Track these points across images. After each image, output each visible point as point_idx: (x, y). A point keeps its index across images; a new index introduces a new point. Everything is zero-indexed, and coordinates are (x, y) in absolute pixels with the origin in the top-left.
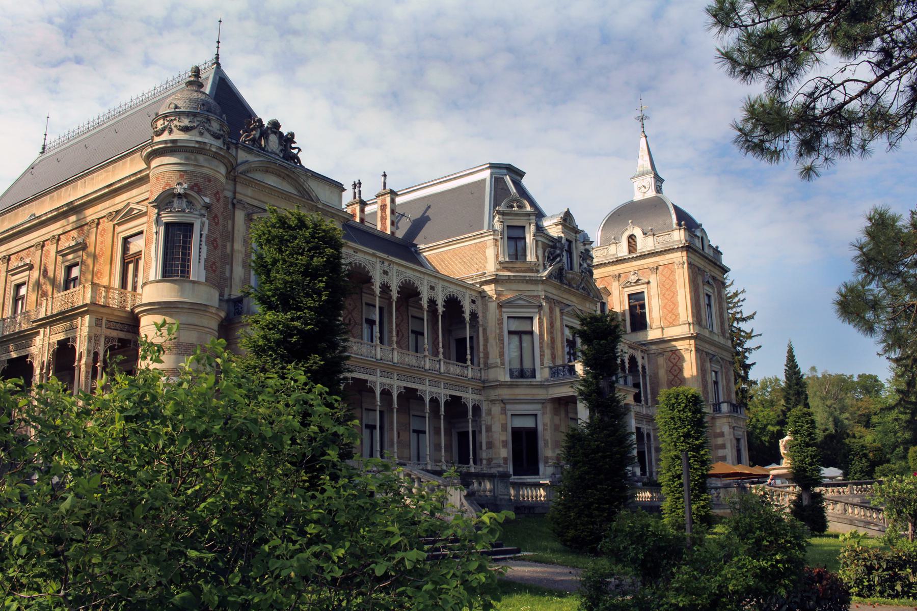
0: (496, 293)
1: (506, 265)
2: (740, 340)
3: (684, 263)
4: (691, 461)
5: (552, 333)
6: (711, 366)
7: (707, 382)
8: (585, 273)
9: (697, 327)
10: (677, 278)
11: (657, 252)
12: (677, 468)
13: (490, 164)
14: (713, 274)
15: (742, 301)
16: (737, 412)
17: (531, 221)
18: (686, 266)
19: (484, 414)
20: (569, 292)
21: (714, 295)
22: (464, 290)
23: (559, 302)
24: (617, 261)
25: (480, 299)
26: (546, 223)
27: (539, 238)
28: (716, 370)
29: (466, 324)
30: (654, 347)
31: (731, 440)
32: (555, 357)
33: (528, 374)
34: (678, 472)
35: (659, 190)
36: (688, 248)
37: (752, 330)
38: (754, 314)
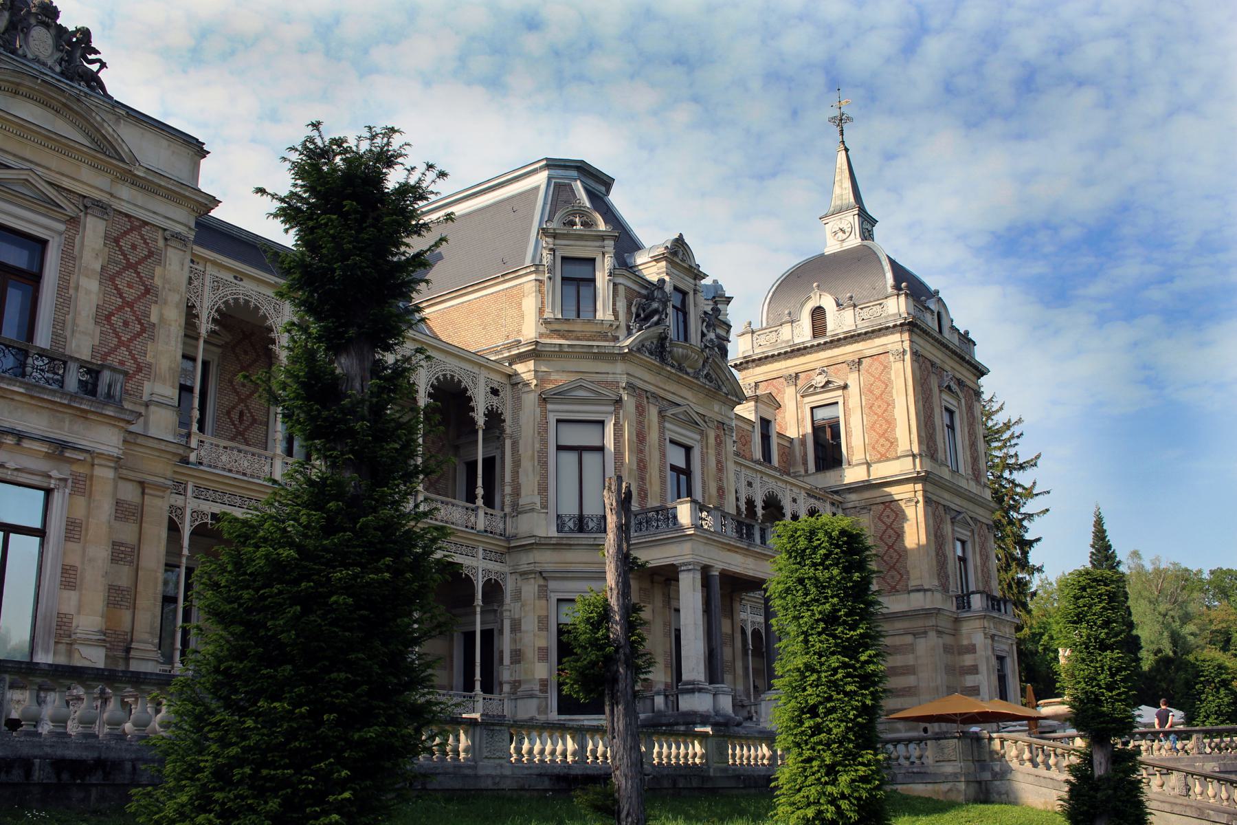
0: (536, 377)
1: (556, 327)
2: (1014, 500)
3: (904, 352)
4: (839, 676)
5: (641, 451)
6: (953, 530)
7: (945, 557)
8: (712, 349)
9: (927, 461)
10: (893, 378)
11: (859, 335)
12: (810, 691)
13: (547, 159)
14: (958, 376)
15: (1018, 437)
16: (999, 610)
17: (606, 249)
18: (908, 357)
19: (508, 599)
20: (679, 381)
21: (960, 412)
22: (476, 370)
23: (655, 396)
24: (792, 351)
25: (508, 387)
26: (641, 259)
27: (619, 280)
28: (964, 538)
29: (477, 431)
30: (853, 497)
32: (646, 495)
33: (591, 525)
34: (811, 702)
35: (867, 234)
36: (911, 326)
37: (1034, 483)
38: (1038, 457)
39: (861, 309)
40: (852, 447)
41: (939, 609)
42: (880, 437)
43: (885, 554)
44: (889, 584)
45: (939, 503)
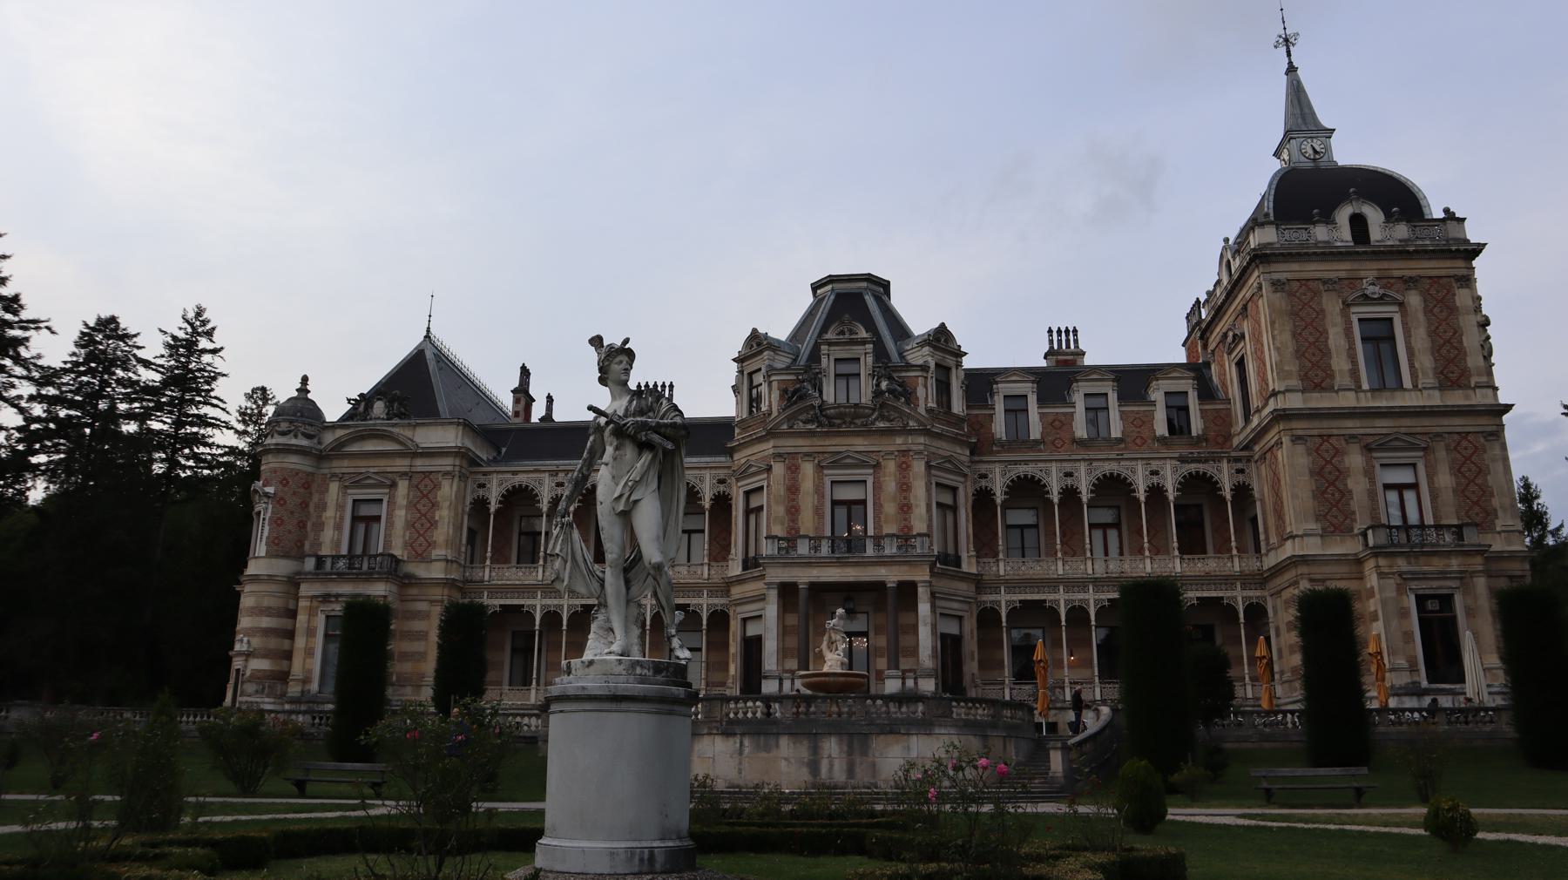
3: (1260, 288)
7: (1346, 494)
30: (1257, 448)
31: (1384, 603)
45: (1330, 436)
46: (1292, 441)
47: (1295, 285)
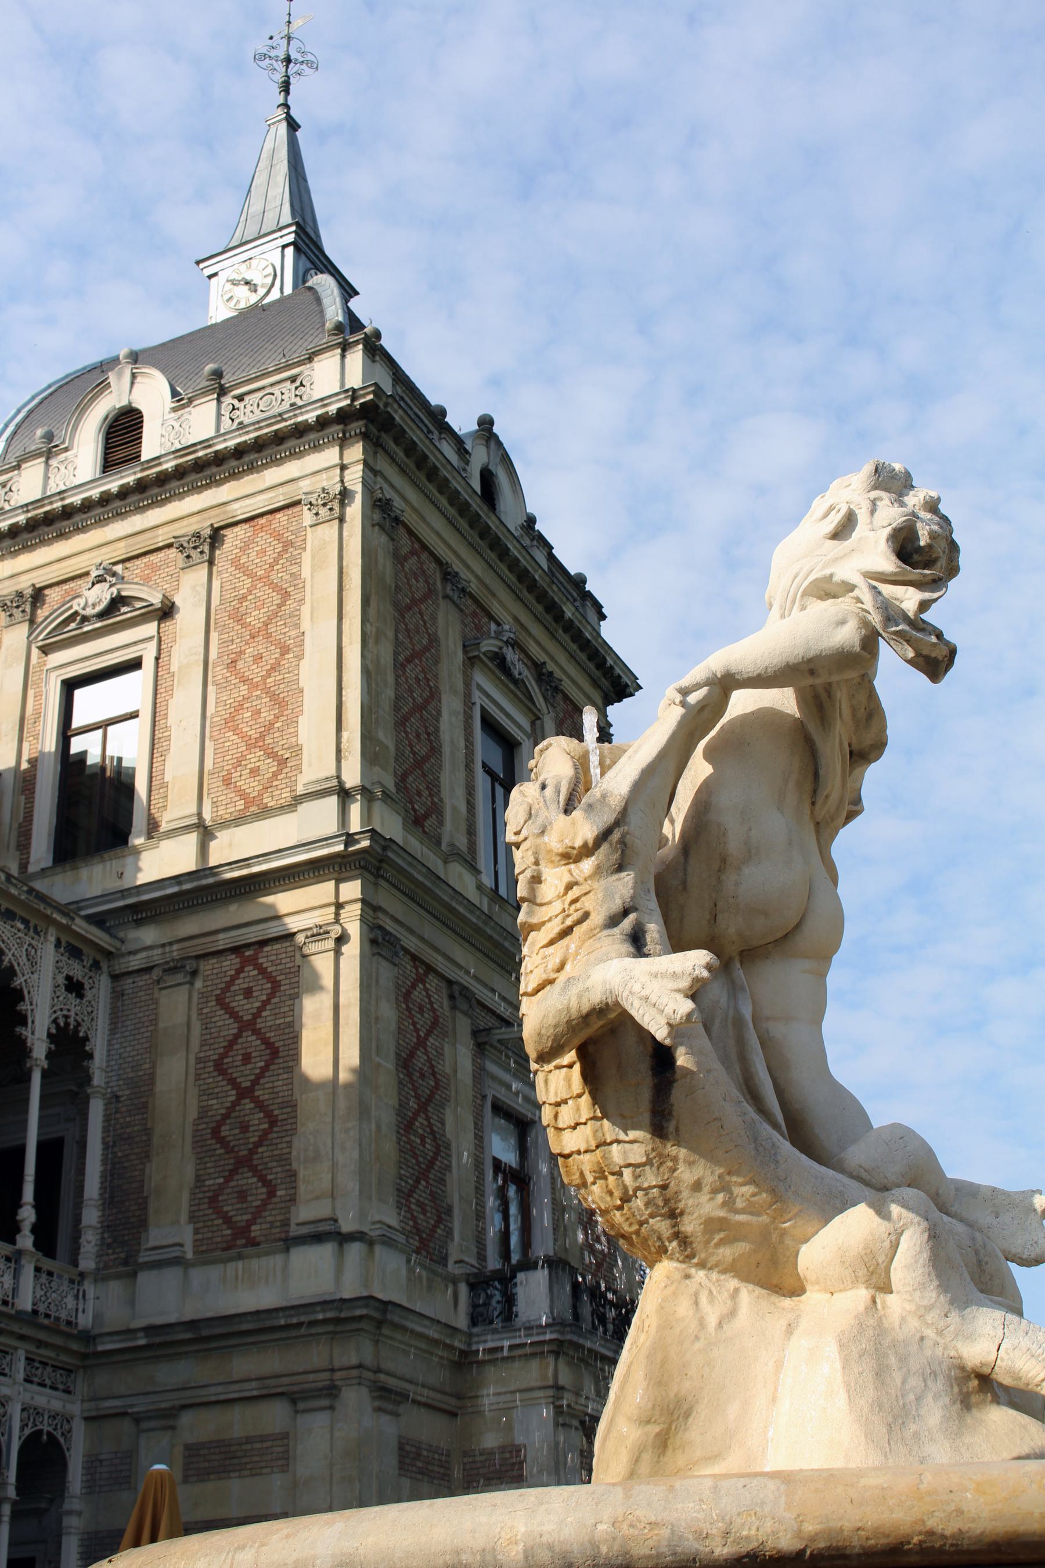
3: (345, 495)
7: (441, 1147)
10: (306, 572)
18: (355, 510)
30: (148, 935)
39: (240, 398)
40: (164, 785)
41: (386, 1305)
42: (250, 747)
43: (226, 1117)
44: (228, 1220)
45: (430, 969)
46: (373, 942)
47: (405, 541)
